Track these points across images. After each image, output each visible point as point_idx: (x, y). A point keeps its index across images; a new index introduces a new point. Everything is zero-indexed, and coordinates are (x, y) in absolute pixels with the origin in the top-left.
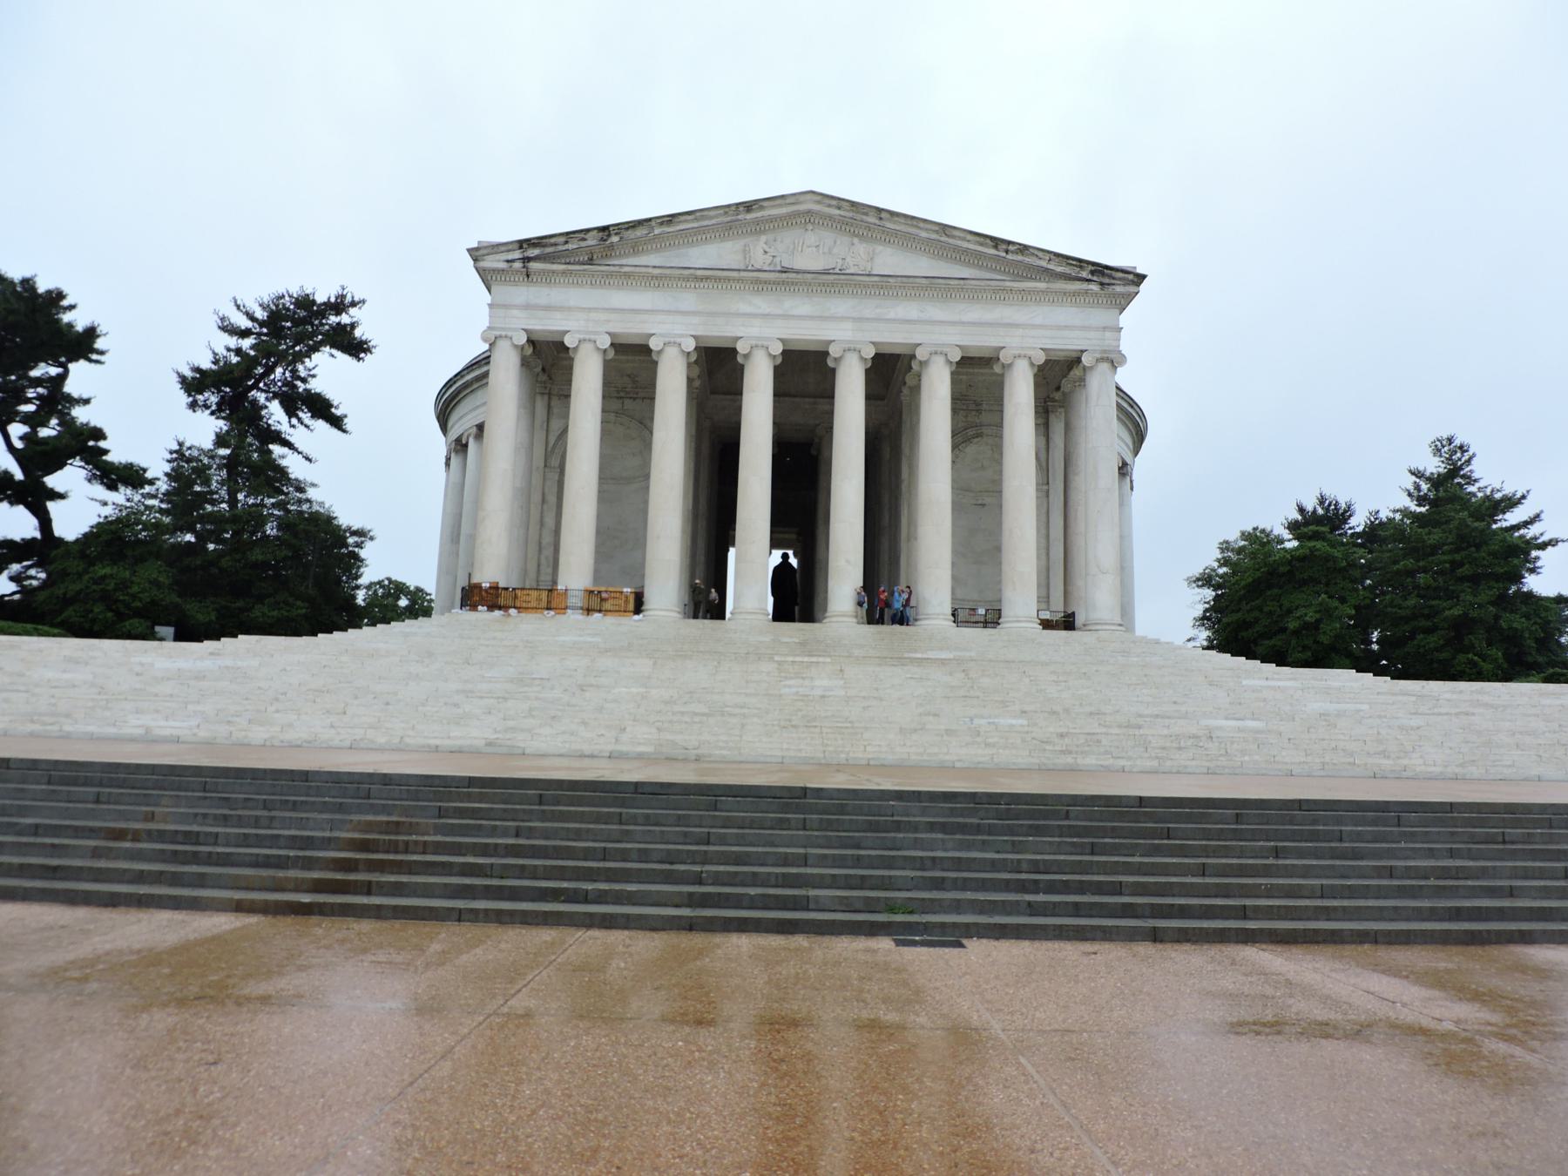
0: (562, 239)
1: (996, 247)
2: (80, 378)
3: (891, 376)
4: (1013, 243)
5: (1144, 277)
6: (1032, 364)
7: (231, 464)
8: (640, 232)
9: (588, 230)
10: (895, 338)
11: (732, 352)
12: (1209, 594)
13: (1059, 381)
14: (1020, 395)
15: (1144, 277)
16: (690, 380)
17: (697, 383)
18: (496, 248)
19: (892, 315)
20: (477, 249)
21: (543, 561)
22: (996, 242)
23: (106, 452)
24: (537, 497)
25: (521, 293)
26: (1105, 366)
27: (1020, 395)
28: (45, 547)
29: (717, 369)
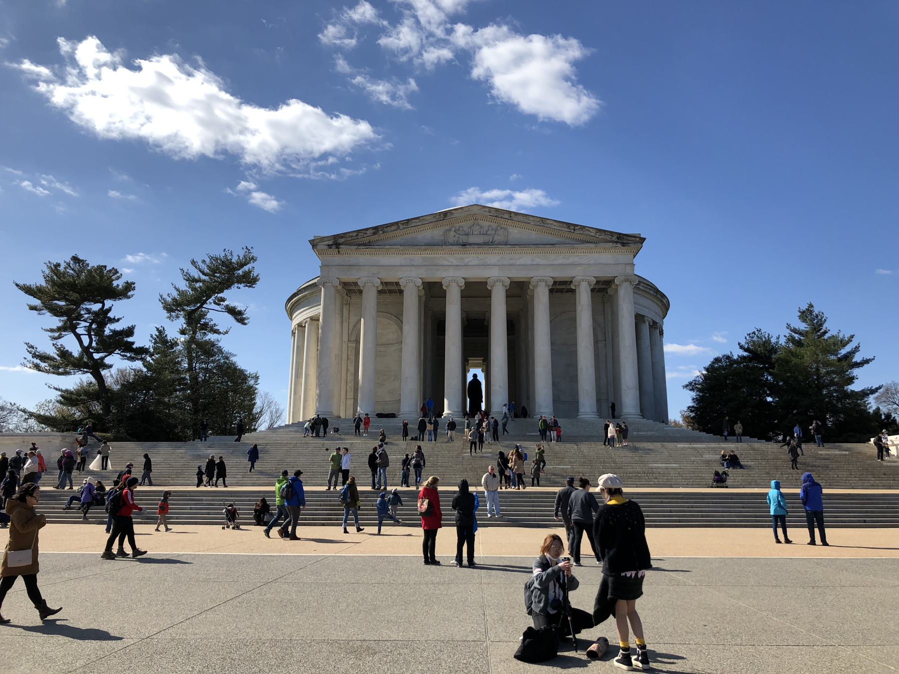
0: (355, 234)
1: (569, 228)
2: (116, 307)
3: (519, 292)
4: (577, 225)
5: (644, 239)
6: (590, 285)
7: (188, 344)
8: (393, 228)
9: (367, 229)
10: (520, 275)
11: (440, 284)
12: (693, 394)
13: (603, 290)
14: (584, 298)
15: (644, 239)
16: (420, 297)
17: (423, 299)
18: (322, 239)
19: (518, 263)
20: (313, 240)
21: (349, 389)
22: (569, 225)
23: (133, 343)
24: (345, 356)
25: (335, 258)
26: (626, 284)
27: (584, 298)
28: (101, 392)
29: (433, 293)
